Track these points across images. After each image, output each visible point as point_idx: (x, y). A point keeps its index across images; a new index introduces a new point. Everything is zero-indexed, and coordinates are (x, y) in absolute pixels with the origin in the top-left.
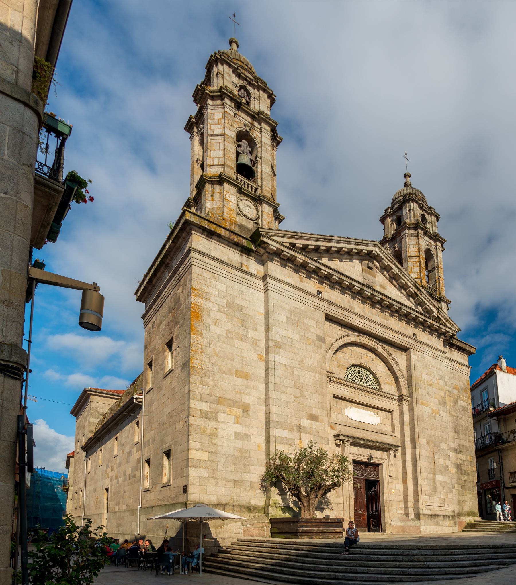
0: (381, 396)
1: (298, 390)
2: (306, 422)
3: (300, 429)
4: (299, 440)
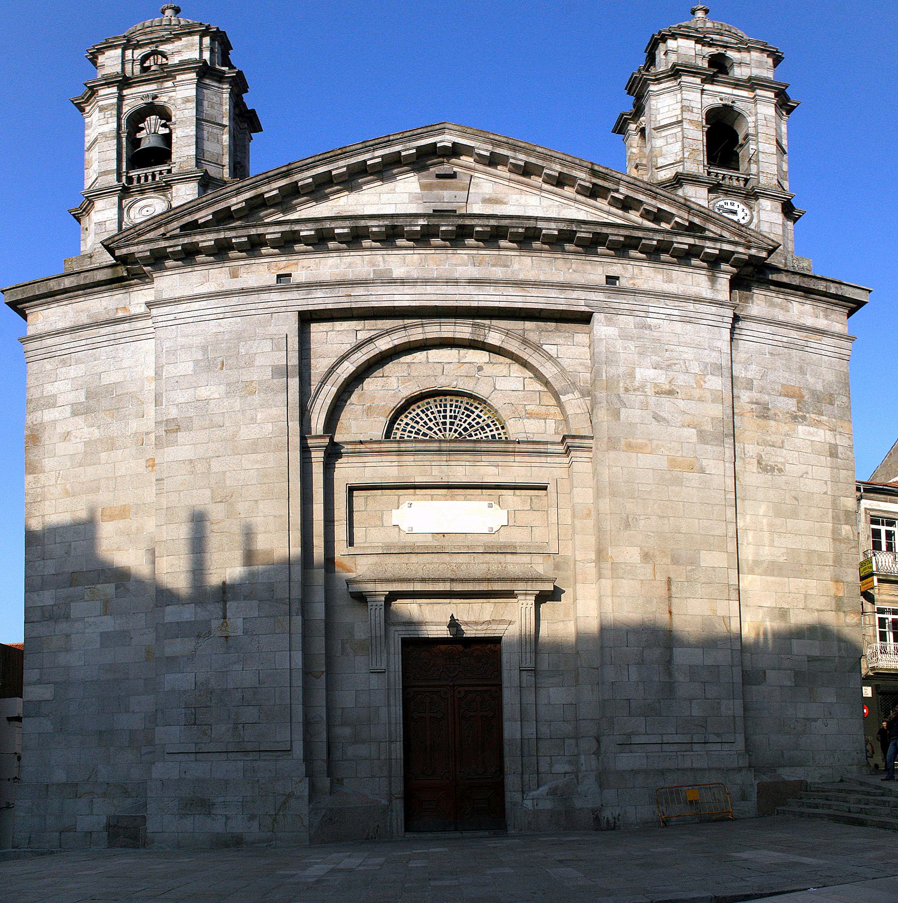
0: (505, 452)
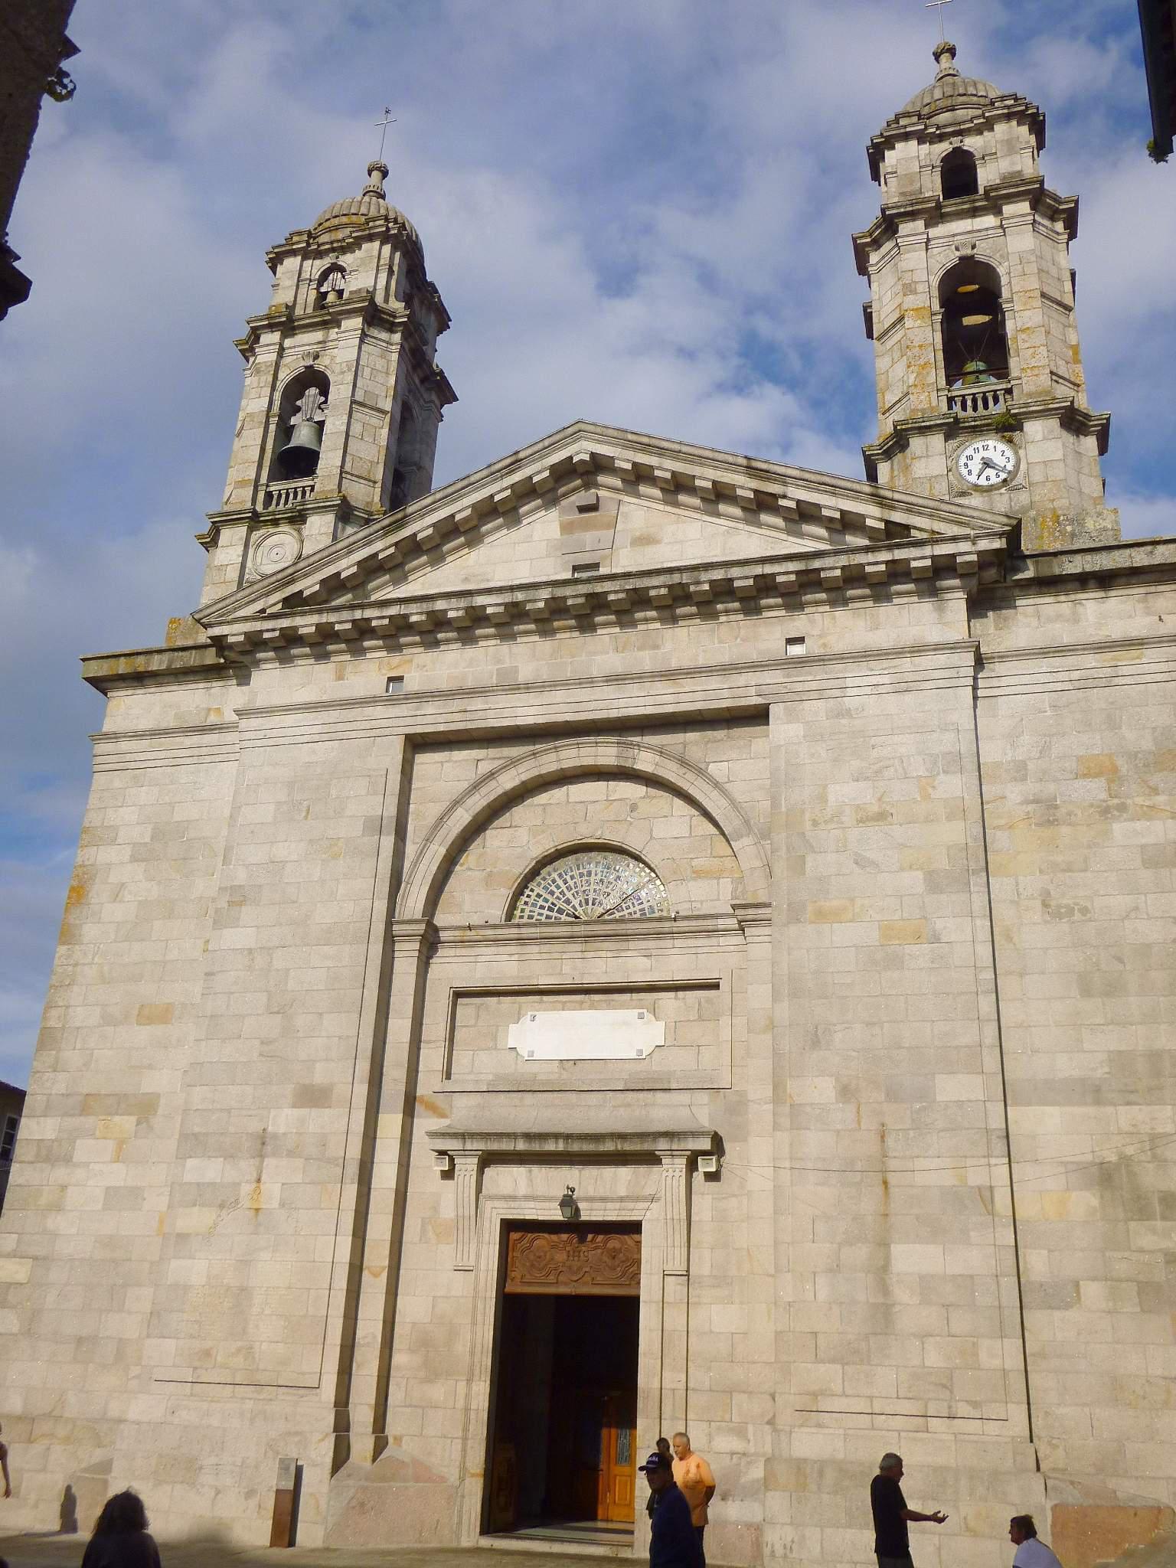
2: (284, 1120)
4: (254, 1185)
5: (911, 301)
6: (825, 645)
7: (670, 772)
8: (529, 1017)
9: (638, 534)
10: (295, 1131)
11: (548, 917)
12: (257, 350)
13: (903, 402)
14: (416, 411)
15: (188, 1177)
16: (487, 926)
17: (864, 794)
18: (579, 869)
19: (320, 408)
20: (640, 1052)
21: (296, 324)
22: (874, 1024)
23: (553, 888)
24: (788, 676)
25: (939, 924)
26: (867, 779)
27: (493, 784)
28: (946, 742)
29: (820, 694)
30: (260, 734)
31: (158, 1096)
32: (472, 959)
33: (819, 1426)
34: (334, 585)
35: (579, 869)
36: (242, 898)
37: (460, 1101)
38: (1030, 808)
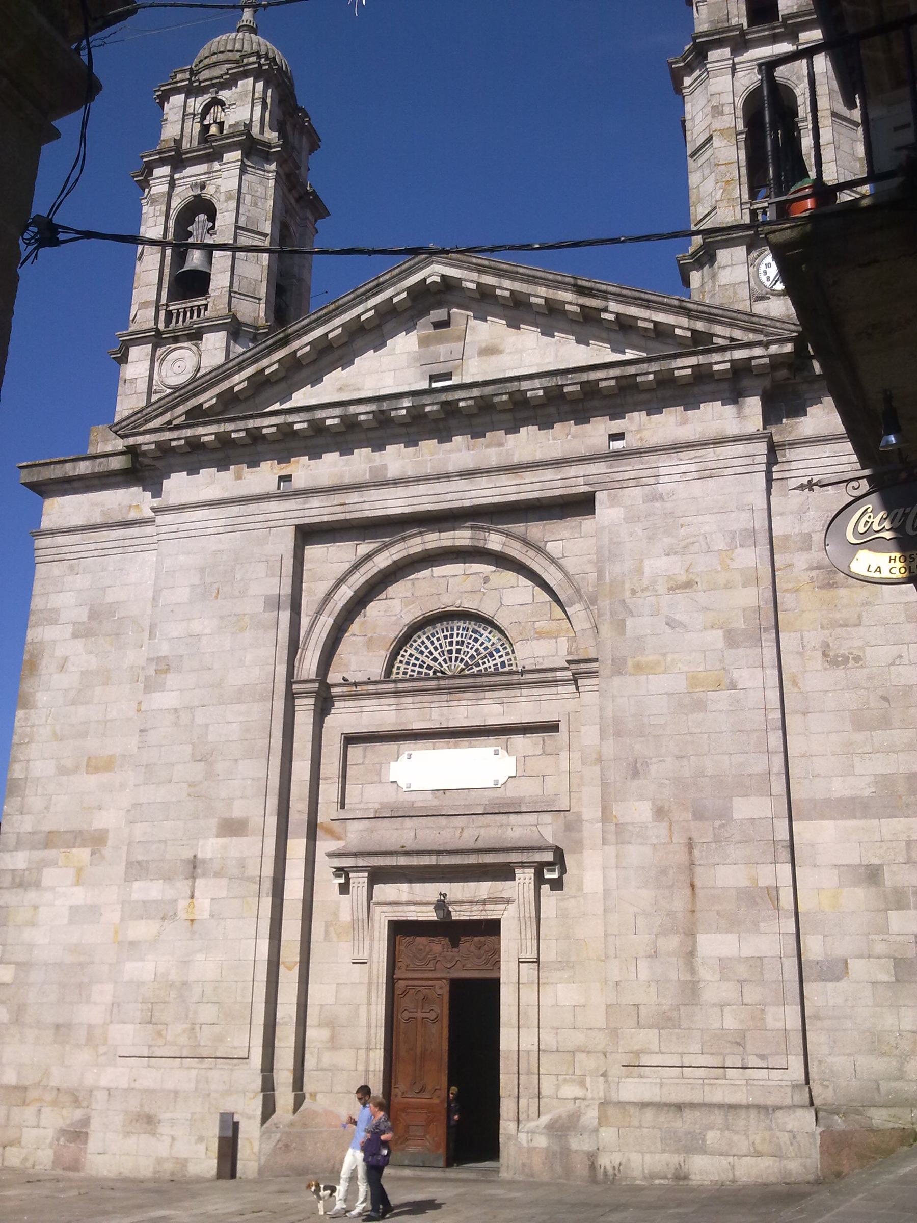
1: (202, 763)
3: (195, 867)
4: (189, 901)
5: (718, 124)
6: (641, 439)
7: (515, 550)
8: (405, 756)
9: (484, 345)
10: (219, 856)
11: (419, 673)
12: (151, 182)
13: (712, 215)
14: (293, 228)
15: (136, 896)
16: (369, 682)
17: (673, 566)
18: (443, 632)
19: (208, 233)
20: (496, 782)
21: (184, 157)
22: (682, 757)
23: (423, 648)
24: (611, 467)
25: (736, 674)
26: (676, 553)
27: (370, 564)
28: (742, 521)
29: (638, 482)
30: (174, 528)
31: (106, 831)
32: (359, 710)
33: (641, 1077)
34: (229, 400)
35: (443, 632)
36: (167, 667)
37: (353, 826)
38: (814, 573)
